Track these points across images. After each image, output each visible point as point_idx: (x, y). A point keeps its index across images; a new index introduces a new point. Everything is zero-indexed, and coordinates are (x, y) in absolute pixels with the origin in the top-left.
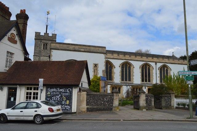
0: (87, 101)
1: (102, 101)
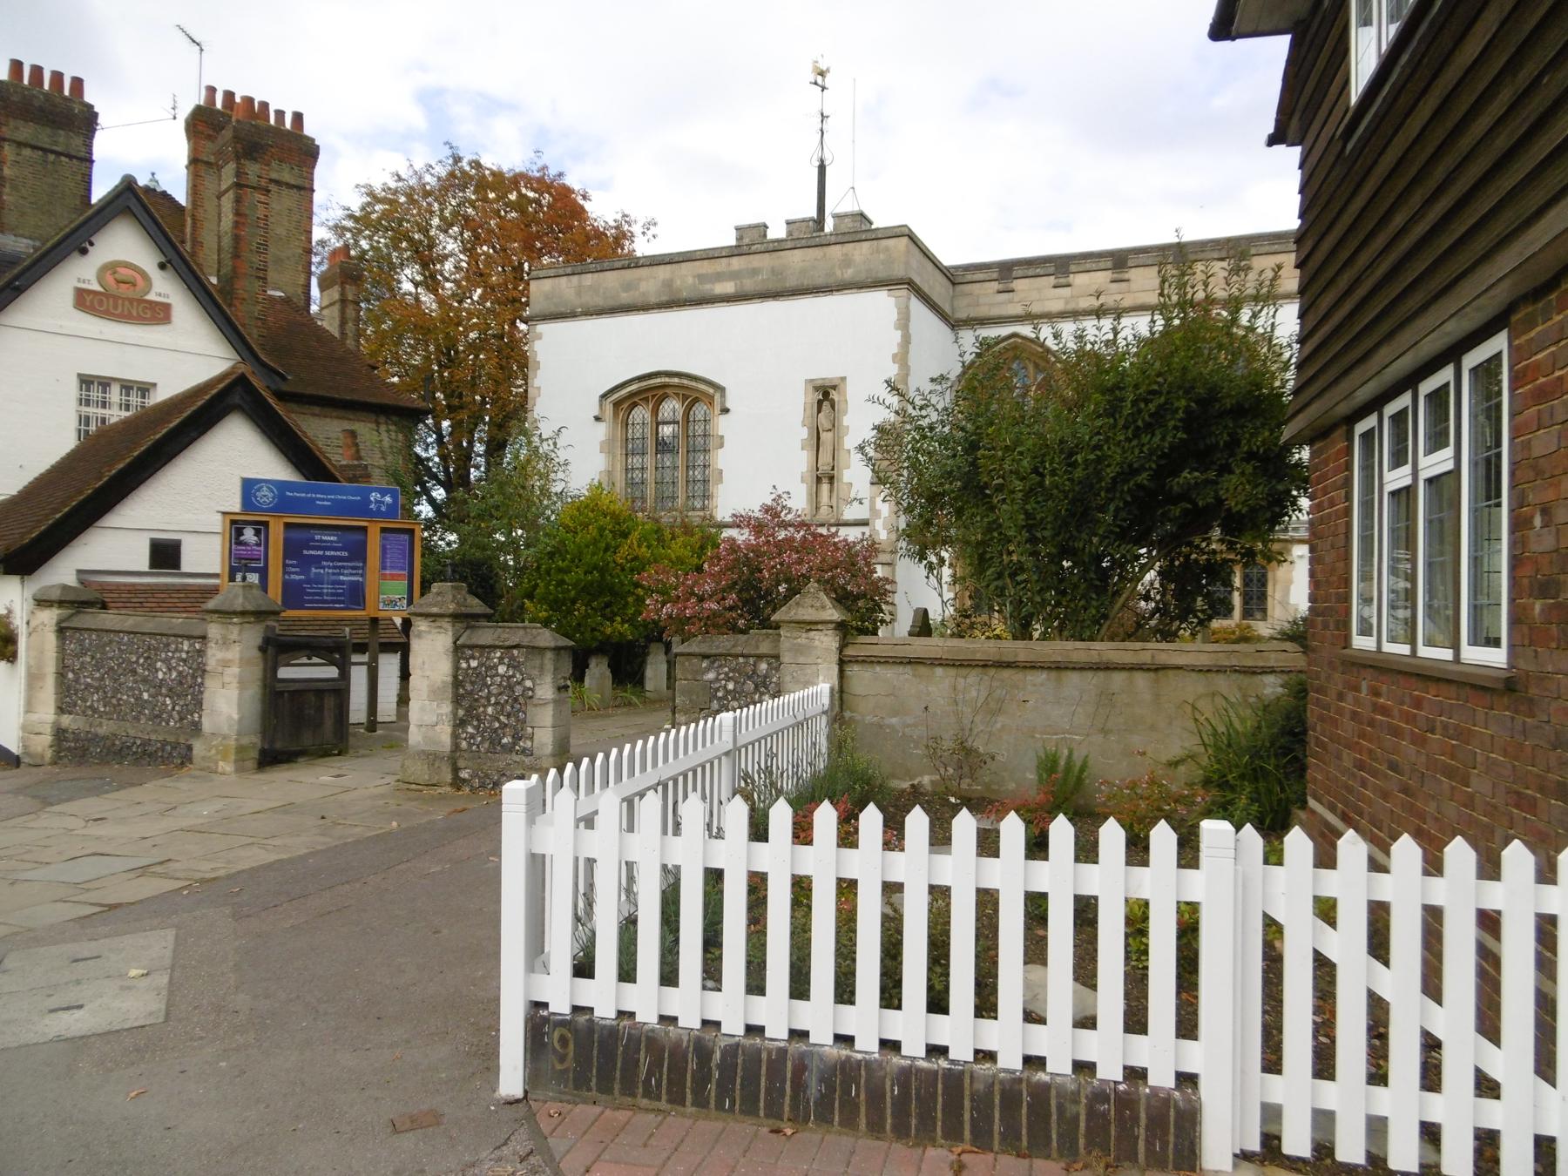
0: (60, 676)
1: (145, 680)
